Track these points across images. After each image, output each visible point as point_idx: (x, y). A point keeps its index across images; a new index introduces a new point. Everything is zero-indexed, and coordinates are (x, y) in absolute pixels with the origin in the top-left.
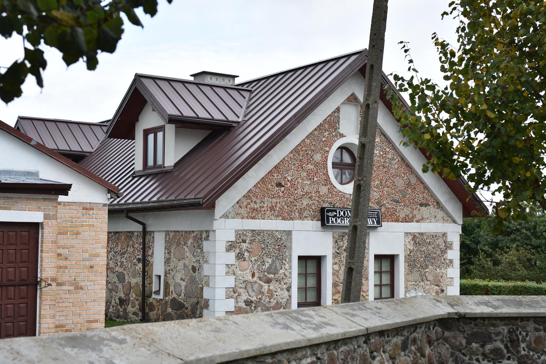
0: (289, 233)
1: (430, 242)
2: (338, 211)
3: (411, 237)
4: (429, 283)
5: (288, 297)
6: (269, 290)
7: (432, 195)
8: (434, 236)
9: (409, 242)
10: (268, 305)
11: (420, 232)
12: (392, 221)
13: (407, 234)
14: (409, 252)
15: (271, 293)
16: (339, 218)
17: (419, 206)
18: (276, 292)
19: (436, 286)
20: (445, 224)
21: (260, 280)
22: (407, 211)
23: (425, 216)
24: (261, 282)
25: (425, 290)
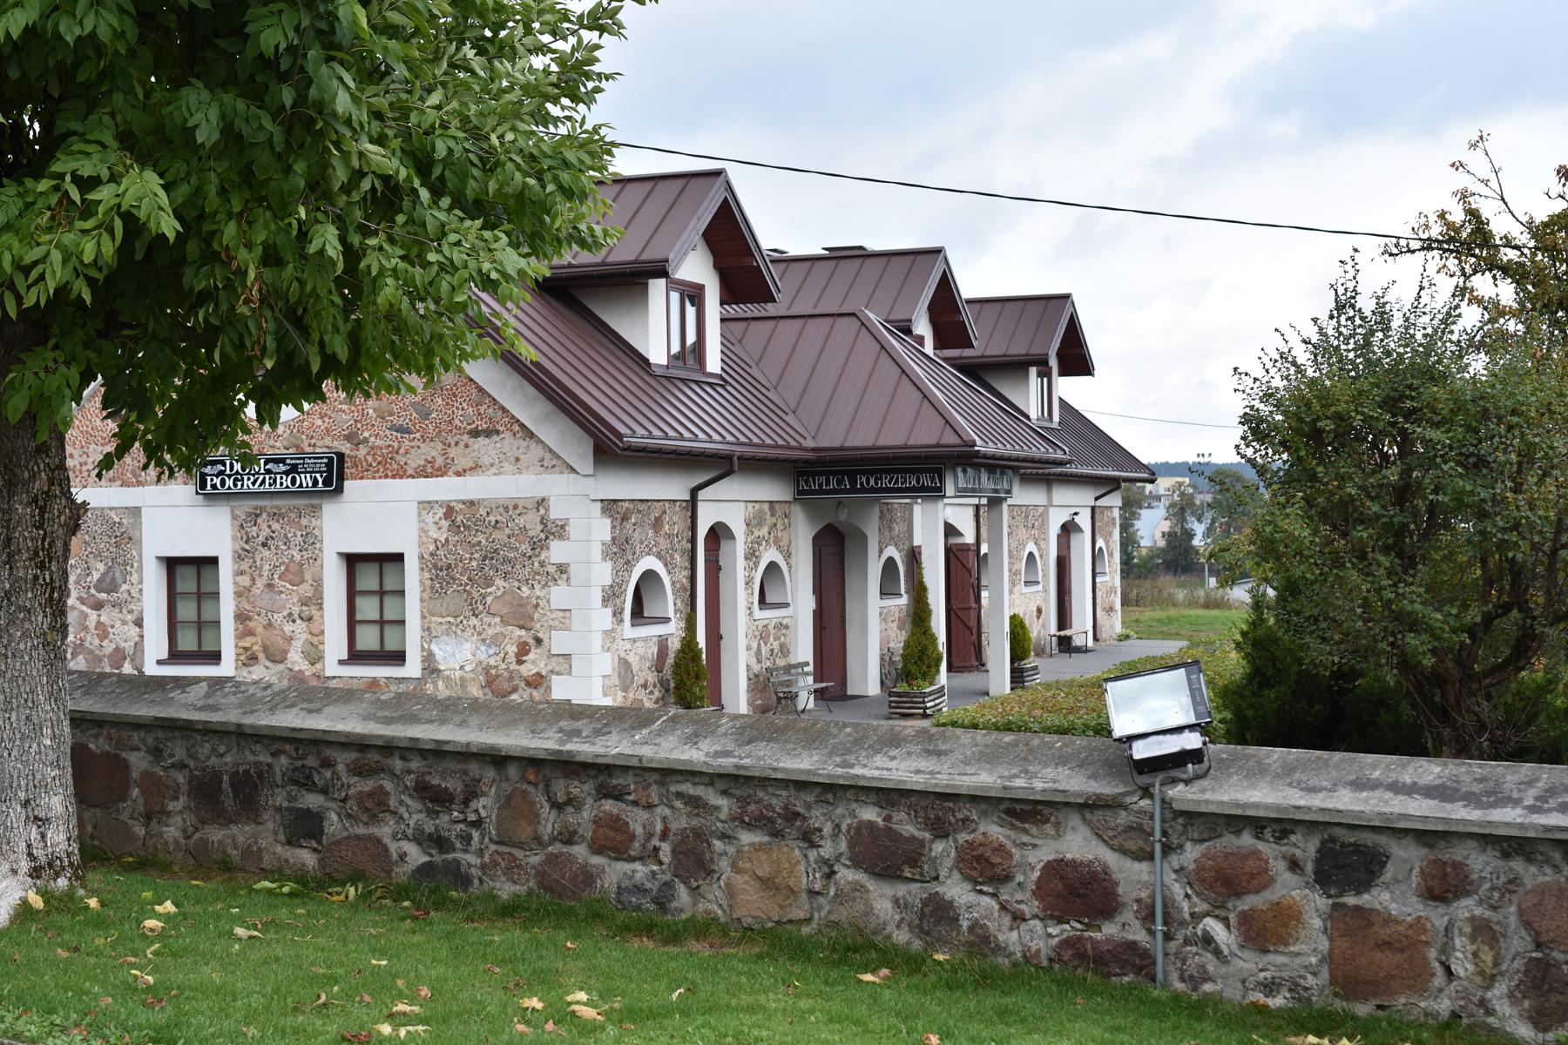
0: (136, 512)
1: (497, 522)
2: (228, 462)
3: (441, 512)
4: (497, 620)
5: (137, 639)
6: (99, 624)
7: (503, 409)
8: (513, 507)
9: (436, 523)
10: (97, 652)
11: (463, 498)
12: (386, 477)
13: (426, 505)
14: (432, 548)
15: (103, 631)
16: (229, 476)
17: (466, 437)
18: (113, 627)
19: (521, 627)
20: (546, 476)
21: (83, 603)
22: (432, 450)
23: (486, 460)
24: (84, 608)
25: (483, 636)
